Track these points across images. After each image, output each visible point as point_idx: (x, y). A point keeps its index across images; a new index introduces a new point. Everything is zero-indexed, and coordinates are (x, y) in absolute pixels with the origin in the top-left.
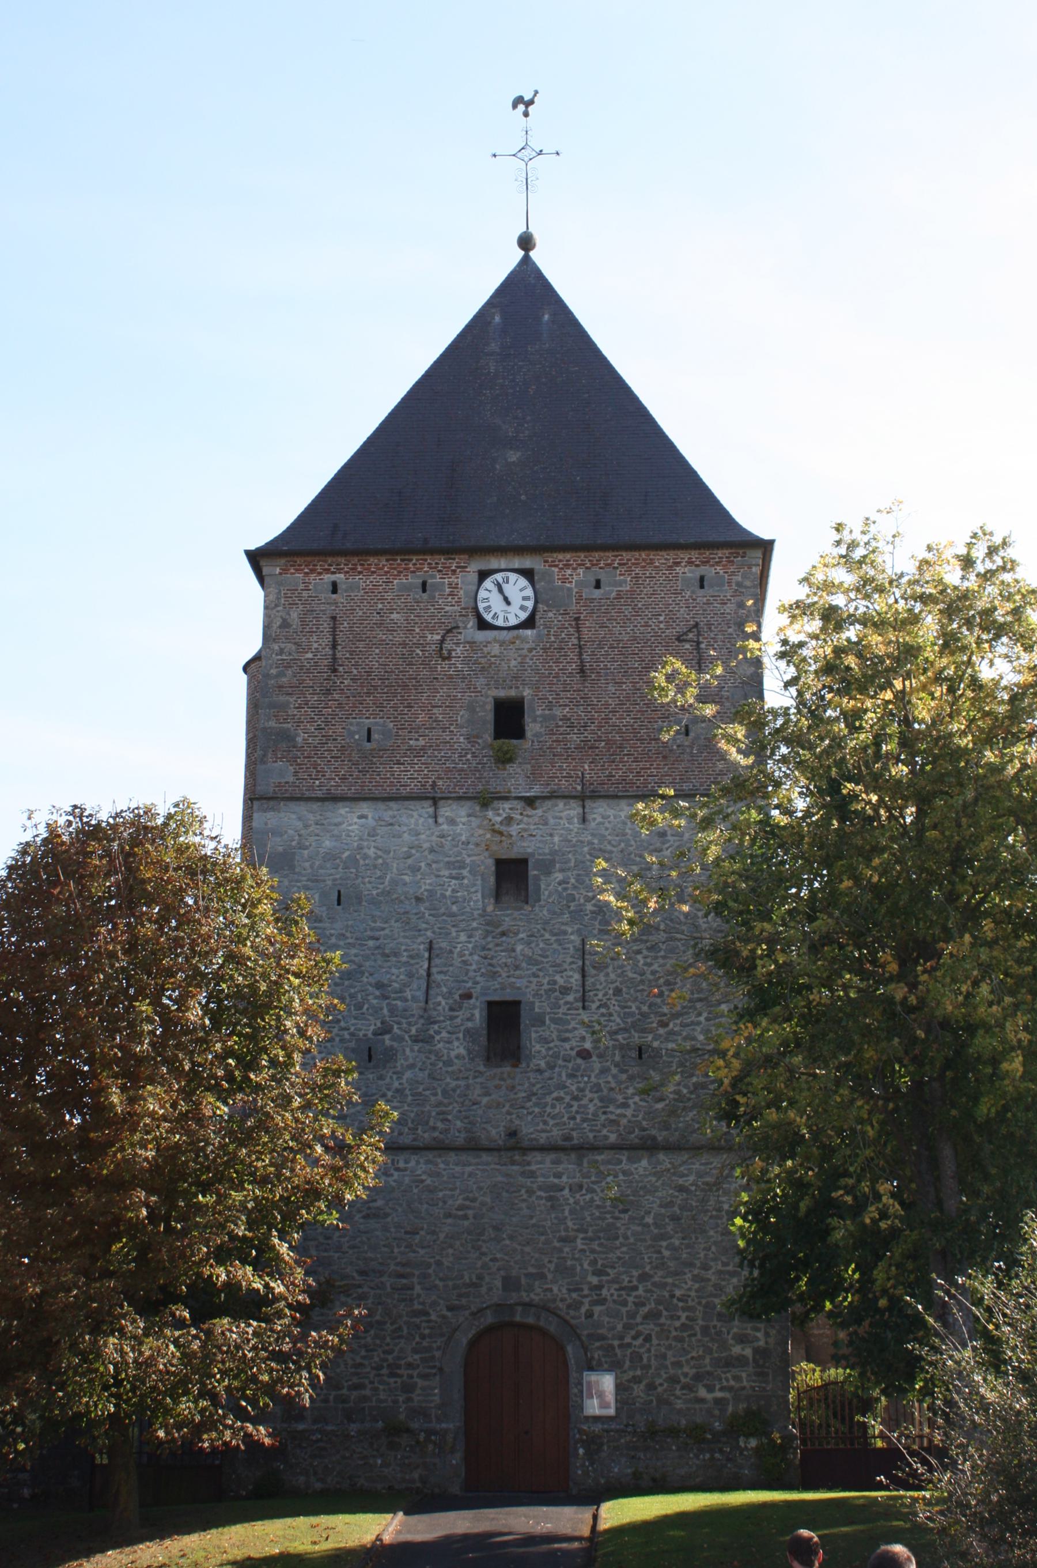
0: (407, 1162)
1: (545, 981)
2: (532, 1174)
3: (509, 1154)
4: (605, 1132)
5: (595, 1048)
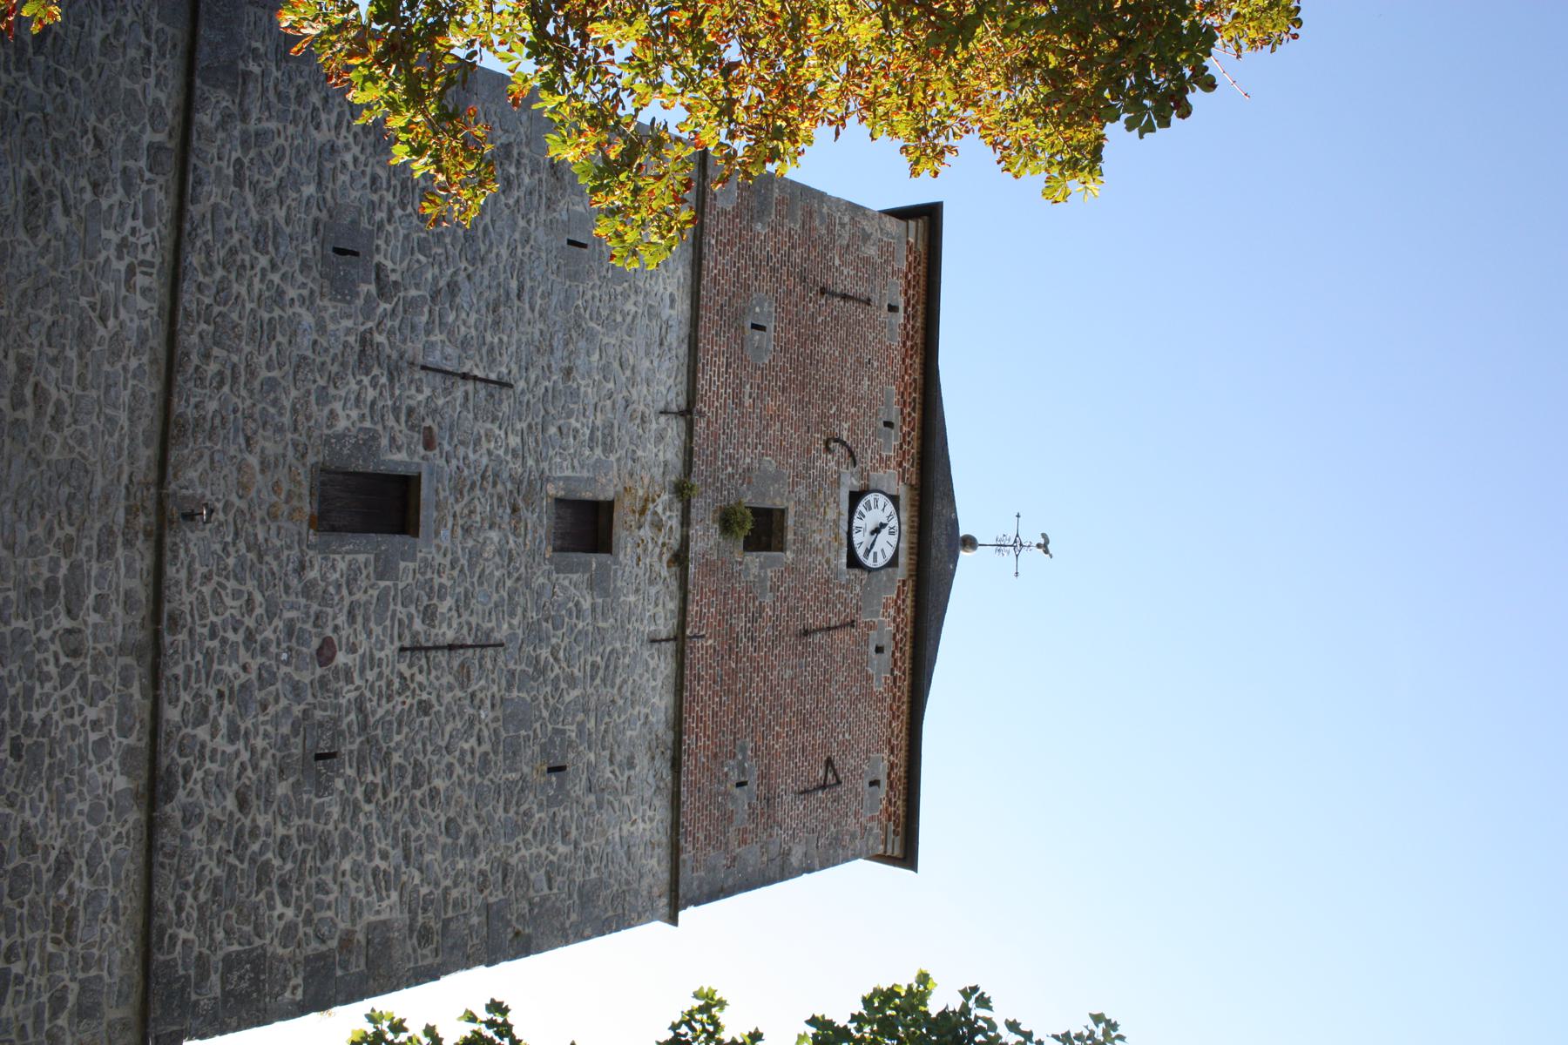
0: (145, 292)
1: (444, 580)
2: (105, 550)
3: (151, 505)
4: (185, 697)
5: (336, 671)
